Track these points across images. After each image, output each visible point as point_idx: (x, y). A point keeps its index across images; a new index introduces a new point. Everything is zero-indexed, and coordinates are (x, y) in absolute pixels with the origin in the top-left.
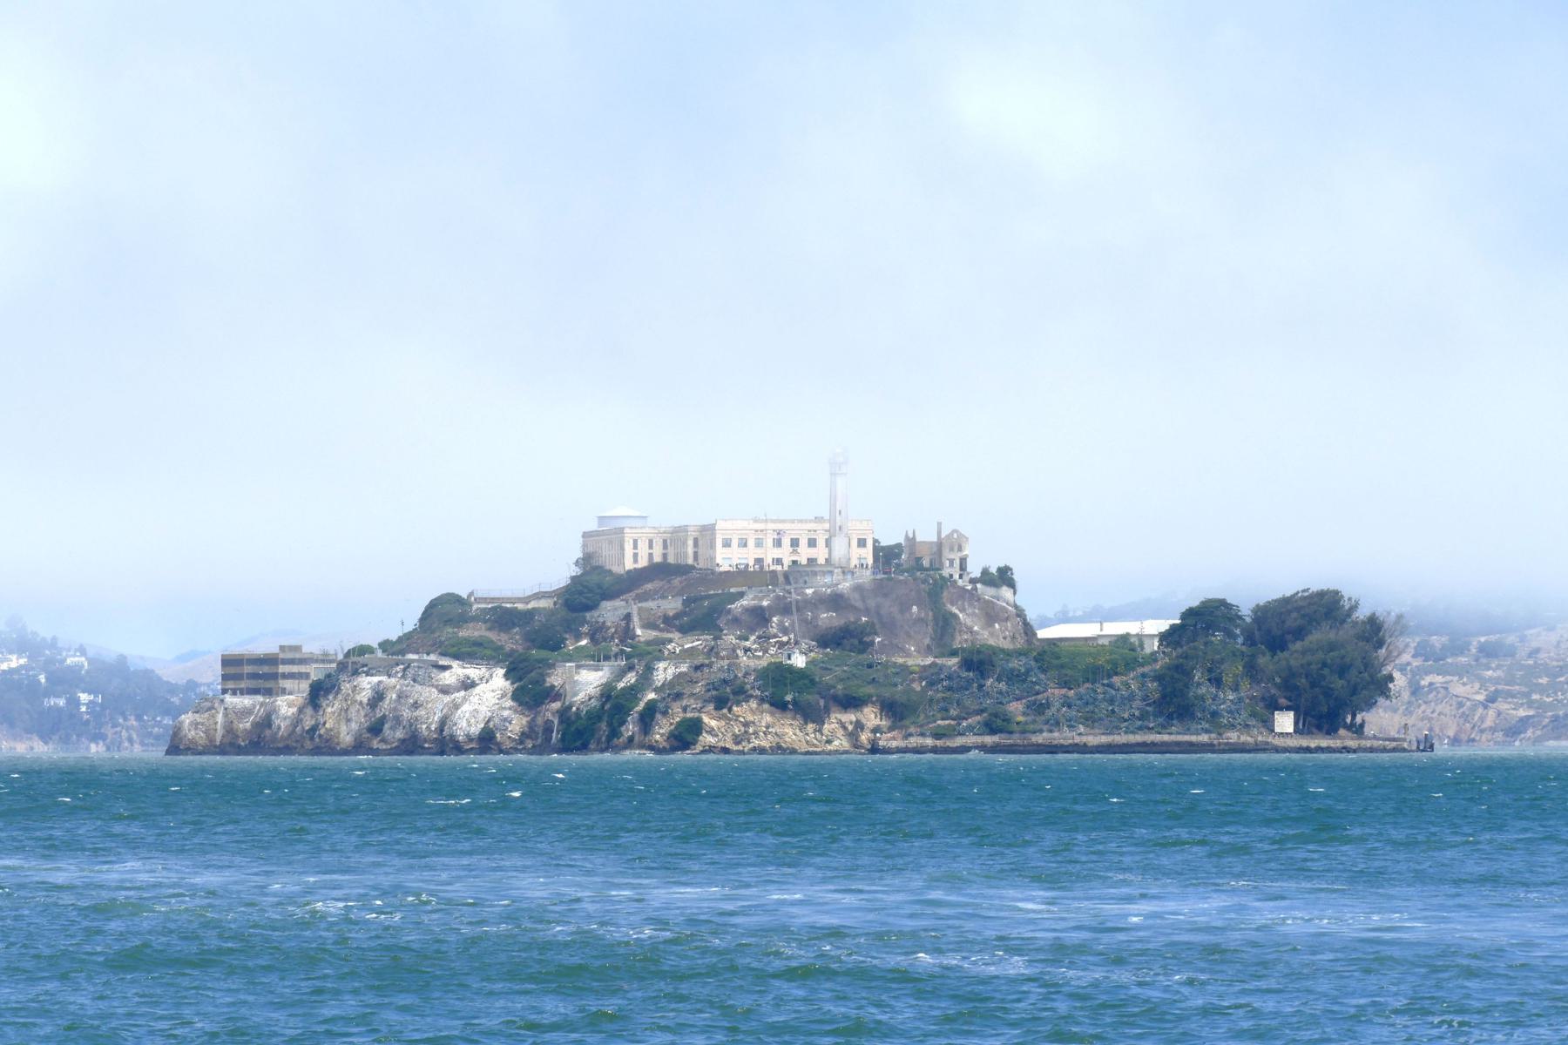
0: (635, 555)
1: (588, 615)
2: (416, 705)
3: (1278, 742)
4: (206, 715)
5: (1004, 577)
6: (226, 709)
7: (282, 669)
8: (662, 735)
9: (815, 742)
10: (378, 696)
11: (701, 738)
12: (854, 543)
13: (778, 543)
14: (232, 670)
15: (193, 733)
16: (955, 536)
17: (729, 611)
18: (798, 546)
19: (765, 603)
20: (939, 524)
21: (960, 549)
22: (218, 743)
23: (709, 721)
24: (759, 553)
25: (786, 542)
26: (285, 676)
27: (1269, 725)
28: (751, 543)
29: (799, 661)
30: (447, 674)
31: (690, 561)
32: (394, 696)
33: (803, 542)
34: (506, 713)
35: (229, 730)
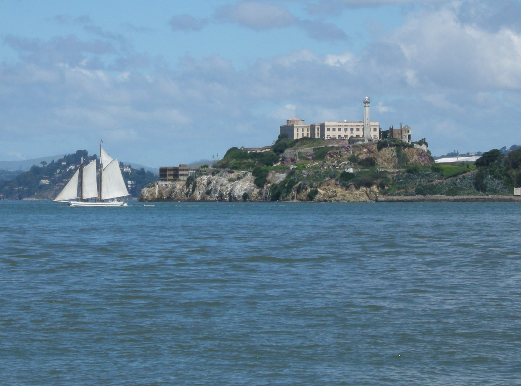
0: (298, 134)
1: (281, 155)
2: (222, 185)
3: (516, 198)
4: (152, 188)
6: (159, 186)
7: (180, 173)
8: (304, 195)
9: (356, 198)
10: (209, 183)
12: (372, 130)
15: (148, 194)
16: (407, 127)
18: (353, 130)
20: (401, 123)
21: (408, 132)
22: (156, 197)
24: (339, 133)
25: (349, 129)
26: (181, 175)
27: (512, 192)
28: (337, 129)
29: (351, 170)
30: (232, 175)
32: (215, 182)
33: (355, 129)
34: (252, 188)
35: (160, 193)
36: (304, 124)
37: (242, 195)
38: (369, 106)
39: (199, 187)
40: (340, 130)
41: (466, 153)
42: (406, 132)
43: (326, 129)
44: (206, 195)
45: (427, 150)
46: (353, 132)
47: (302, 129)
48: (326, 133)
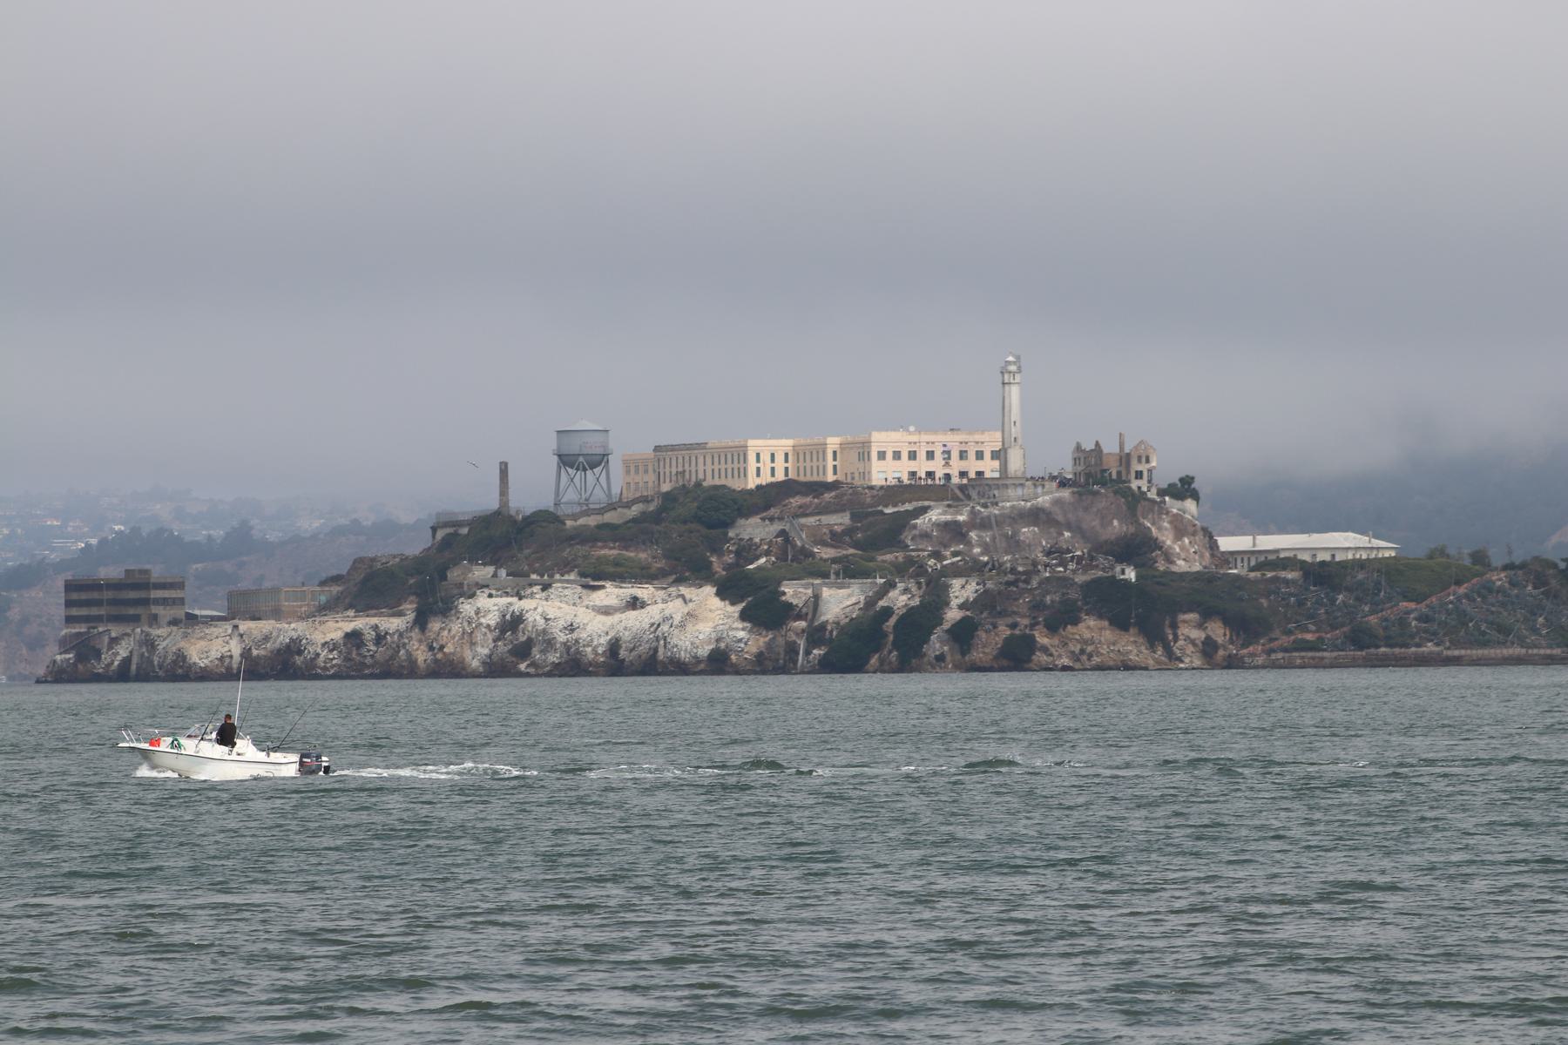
5: (1184, 488)
10: (512, 623)
11: (1034, 657)
14: (75, 596)
16: (1143, 447)
17: (915, 527)
18: (949, 458)
19: (961, 518)
20: (1120, 434)
21: (1148, 461)
23: (1042, 639)
24: (914, 466)
26: (157, 602)
28: (905, 455)
31: (830, 478)
33: (955, 455)
34: (741, 634)
35: (246, 654)
40: (913, 456)
41: (430, 531)
42: (1139, 458)
43: (874, 455)
44: (514, 659)
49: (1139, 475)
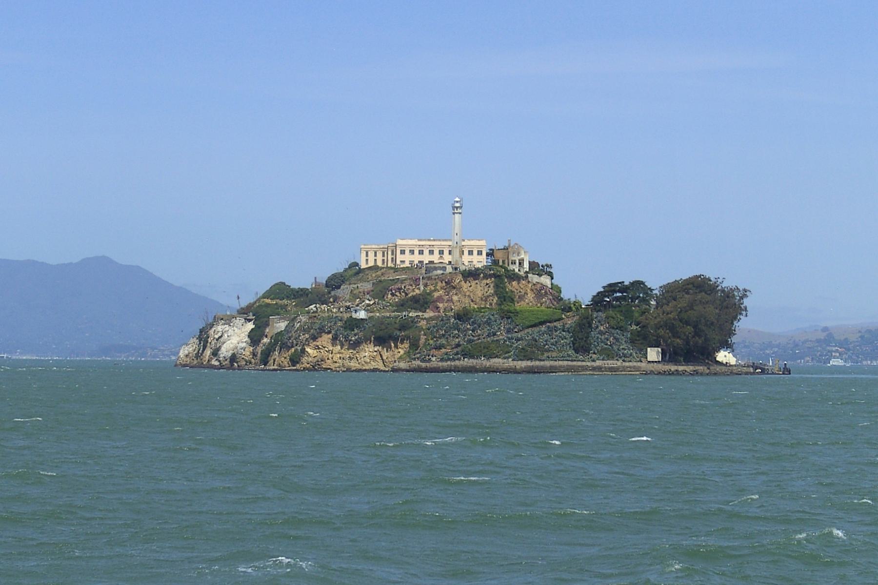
0: (367, 260)
12: (466, 253)
13: (431, 252)
18: (443, 254)
24: (421, 258)
25: (436, 252)
27: (645, 355)
28: (416, 252)
33: (446, 252)
34: (244, 345)
36: (378, 245)
37: (230, 356)
38: (460, 213)
39: (210, 343)
40: (421, 252)
43: (398, 252)
45: (552, 284)
46: (443, 257)
47: (374, 252)
48: (400, 257)
49: (514, 263)
